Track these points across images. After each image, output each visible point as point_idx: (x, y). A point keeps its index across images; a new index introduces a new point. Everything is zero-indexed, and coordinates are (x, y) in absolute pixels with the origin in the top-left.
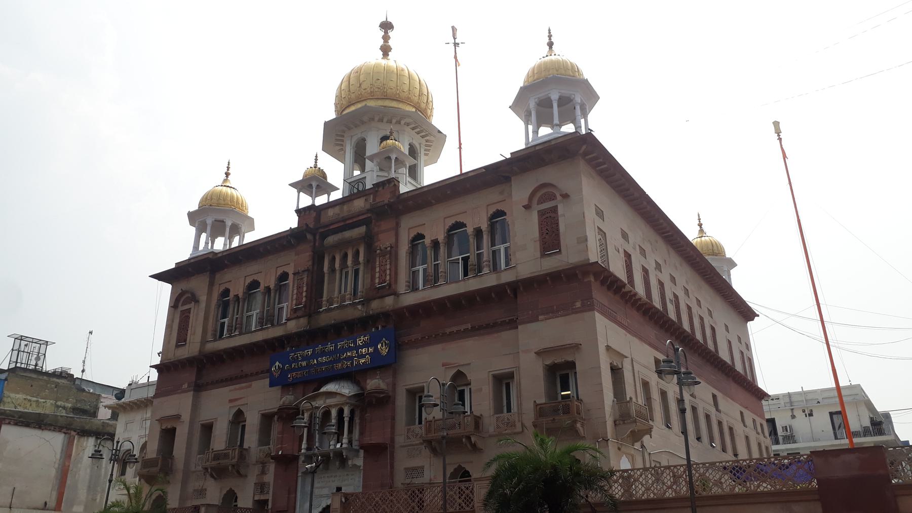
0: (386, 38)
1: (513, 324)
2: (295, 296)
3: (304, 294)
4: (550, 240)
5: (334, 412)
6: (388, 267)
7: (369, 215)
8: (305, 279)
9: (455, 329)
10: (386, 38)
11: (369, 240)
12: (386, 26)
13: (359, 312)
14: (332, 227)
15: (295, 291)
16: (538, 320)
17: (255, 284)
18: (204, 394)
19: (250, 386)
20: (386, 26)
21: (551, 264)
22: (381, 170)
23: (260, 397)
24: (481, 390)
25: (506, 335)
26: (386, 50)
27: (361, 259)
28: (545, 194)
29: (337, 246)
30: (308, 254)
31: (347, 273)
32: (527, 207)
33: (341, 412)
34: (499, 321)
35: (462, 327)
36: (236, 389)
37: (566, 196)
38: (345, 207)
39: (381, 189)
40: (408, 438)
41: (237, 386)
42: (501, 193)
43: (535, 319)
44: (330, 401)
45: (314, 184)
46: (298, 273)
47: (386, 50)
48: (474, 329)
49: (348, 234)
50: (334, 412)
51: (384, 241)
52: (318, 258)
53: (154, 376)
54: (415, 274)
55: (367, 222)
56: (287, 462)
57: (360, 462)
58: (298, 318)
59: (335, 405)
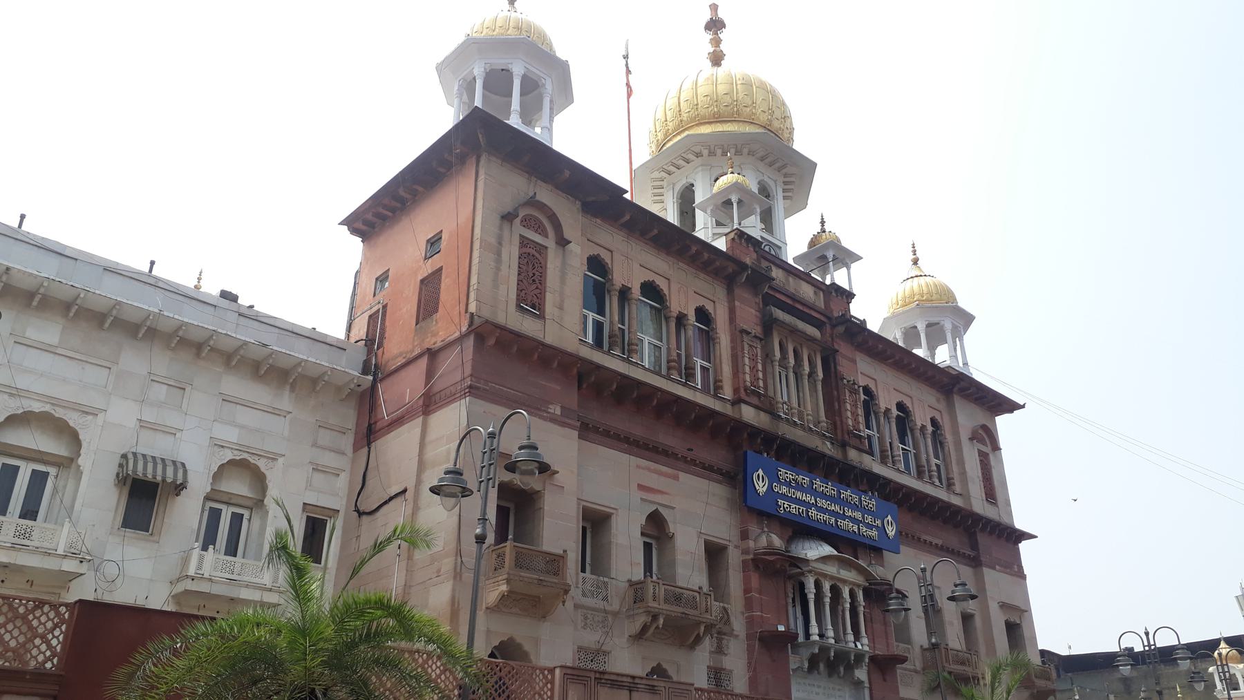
0: (717, 42)
7: (822, 318)
9: (929, 538)
13: (828, 448)
14: (778, 295)
16: (994, 568)
17: (650, 290)
19: (676, 478)
20: (715, 25)
22: (719, 224)
23: (699, 510)
24: (952, 624)
26: (717, 59)
29: (794, 331)
35: (935, 541)
36: (649, 469)
38: (791, 279)
42: (938, 400)
45: (734, 199)
47: (717, 59)
49: (801, 325)
51: (844, 367)
56: (772, 645)
59: (851, 583)
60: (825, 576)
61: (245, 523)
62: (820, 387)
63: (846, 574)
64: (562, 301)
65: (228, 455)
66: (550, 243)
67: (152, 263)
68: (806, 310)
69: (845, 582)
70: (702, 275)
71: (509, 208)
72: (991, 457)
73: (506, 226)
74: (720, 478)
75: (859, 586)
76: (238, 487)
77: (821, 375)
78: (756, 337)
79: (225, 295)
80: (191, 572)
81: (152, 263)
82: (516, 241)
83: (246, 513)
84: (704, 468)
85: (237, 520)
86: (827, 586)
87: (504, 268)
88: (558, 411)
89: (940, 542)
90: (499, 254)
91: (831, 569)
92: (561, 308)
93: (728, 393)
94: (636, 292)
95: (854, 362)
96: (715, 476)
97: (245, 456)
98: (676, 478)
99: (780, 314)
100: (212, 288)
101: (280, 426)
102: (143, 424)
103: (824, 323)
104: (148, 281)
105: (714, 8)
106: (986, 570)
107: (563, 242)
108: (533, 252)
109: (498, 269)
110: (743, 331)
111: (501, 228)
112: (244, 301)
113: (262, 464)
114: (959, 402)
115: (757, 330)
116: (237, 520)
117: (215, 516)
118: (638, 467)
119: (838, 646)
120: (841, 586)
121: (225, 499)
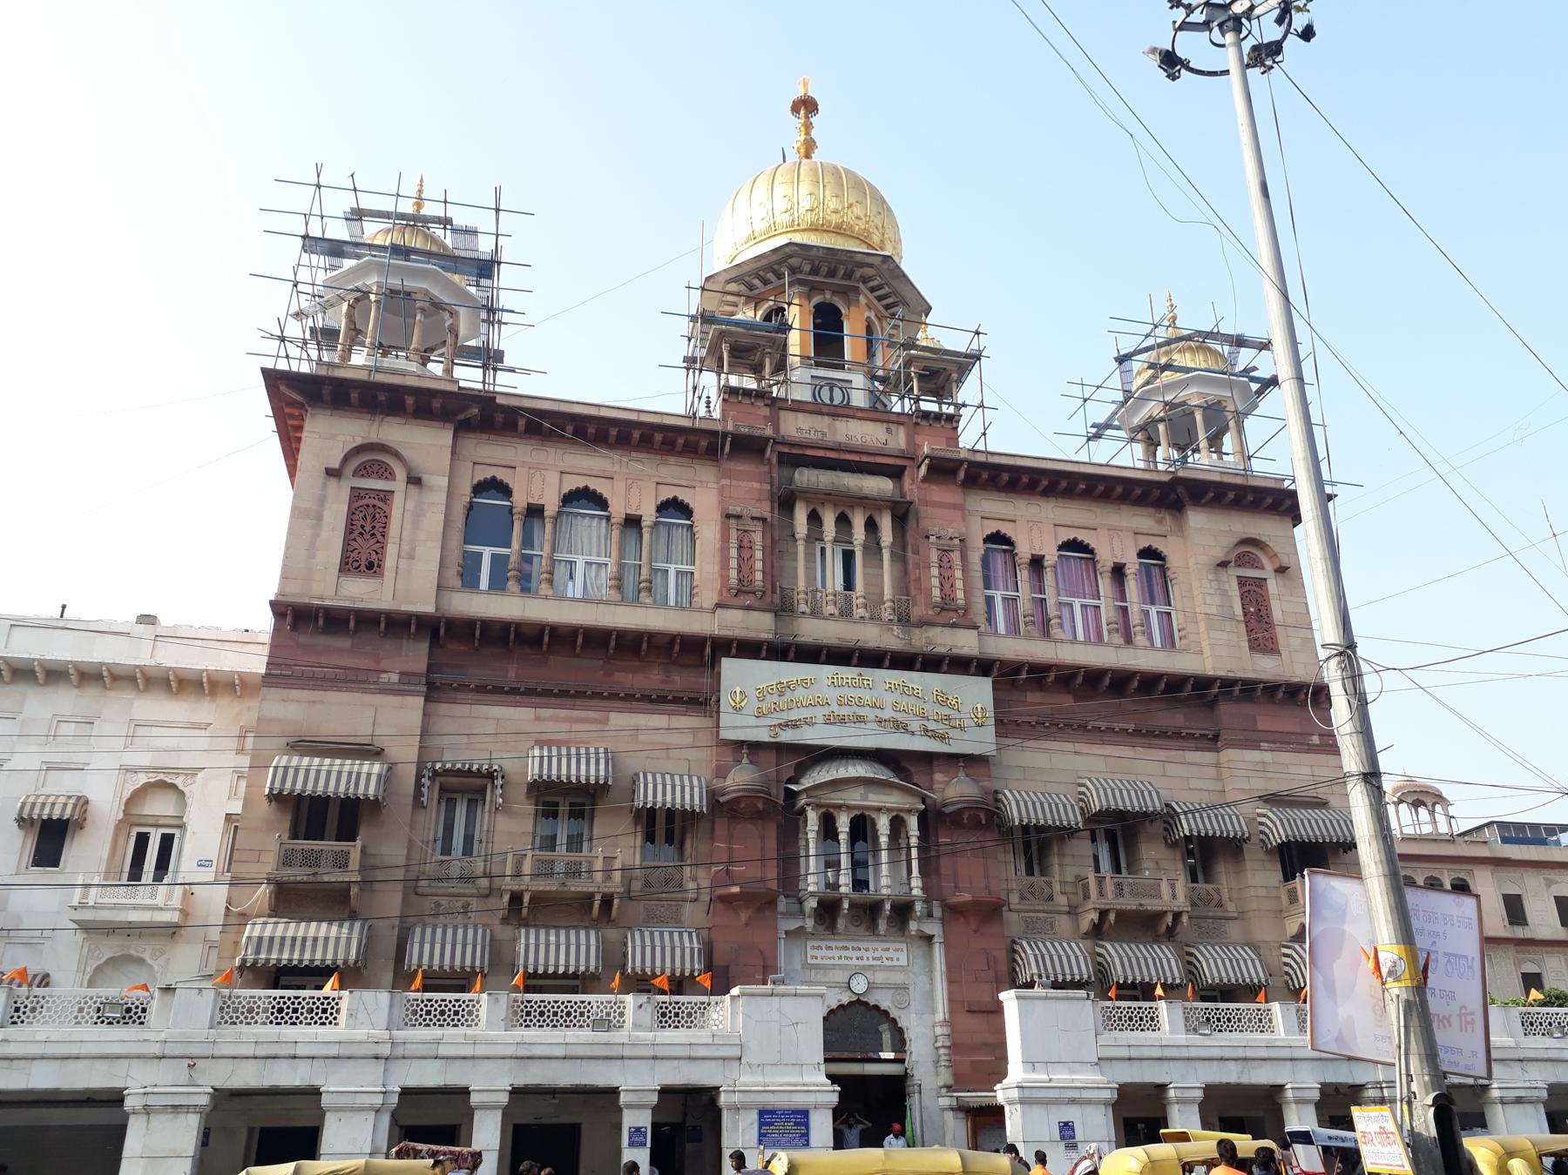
1: (1212, 741)
2: (734, 563)
3: (759, 565)
4: (1260, 628)
5: (883, 824)
6: (958, 574)
7: (900, 462)
8: (757, 537)
10: (808, 127)
11: (902, 514)
12: (806, 106)
14: (809, 452)
15: (734, 552)
18: (444, 708)
21: (1265, 668)
25: (1207, 757)
27: (886, 535)
28: (1244, 554)
30: (756, 485)
31: (823, 550)
32: (1223, 565)
33: (897, 824)
34: (1184, 732)
36: (555, 719)
37: (1282, 570)
39: (924, 423)
40: (1022, 898)
41: (563, 713)
42: (1160, 522)
43: (1254, 745)
44: (874, 799)
46: (739, 517)
48: (1137, 732)
50: (883, 824)
52: (785, 502)
53: (265, 622)
54: (989, 601)
55: (896, 473)
57: (934, 928)
58: (749, 608)
59: (889, 810)
60: (839, 807)
61: (176, 841)
62: (886, 555)
63: (894, 800)
64: (414, 549)
65: (143, 779)
66: (398, 485)
67: (64, 607)
68: (865, 459)
69: (879, 809)
70: (672, 459)
71: (335, 464)
72: (1273, 586)
73: (333, 482)
74: (682, 708)
75: (909, 811)
76: (159, 806)
77: (886, 535)
78: (753, 518)
79: (147, 619)
80: (75, 903)
81: (64, 607)
82: (345, 495)
83: (176, 832)
84: (652, 701)
85: (167, 841)
86: (843, 823)
87: (325, 534)
88: (395, 678)
89: (1131, 727)
90: (319, 518)
91: (855, 797)
92: (411, 557)
93: (708, 597)
94: (552, 505)
95: (960, 508)
96: (672, 707)
97: (161, 777)
98: (606, 721)
99: (805, 477)
100: (125, 616)
101: (200, 741)
102: (50, 768)
103: (904, 468)
104: (61, 624)
105: (805, 84)
106: (1229, 755)
107: (415, 481)
108: (372, 502)
109: (316, 536)
110: (728, 516)
111: (324, 486)
112: (166, 620)
113: (179, 782)
114: (1196, 519)
115: (764, 509)
116: (167, 841)
117: (142, 840)
118: (537, 719)
119: (856, 896)
120: (874, 815)
121: (151, 821)
